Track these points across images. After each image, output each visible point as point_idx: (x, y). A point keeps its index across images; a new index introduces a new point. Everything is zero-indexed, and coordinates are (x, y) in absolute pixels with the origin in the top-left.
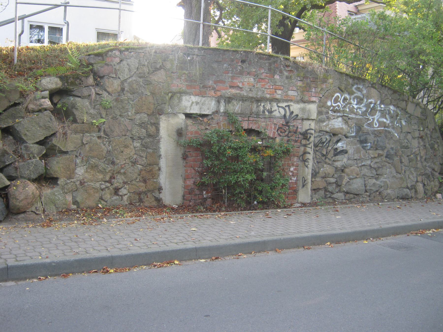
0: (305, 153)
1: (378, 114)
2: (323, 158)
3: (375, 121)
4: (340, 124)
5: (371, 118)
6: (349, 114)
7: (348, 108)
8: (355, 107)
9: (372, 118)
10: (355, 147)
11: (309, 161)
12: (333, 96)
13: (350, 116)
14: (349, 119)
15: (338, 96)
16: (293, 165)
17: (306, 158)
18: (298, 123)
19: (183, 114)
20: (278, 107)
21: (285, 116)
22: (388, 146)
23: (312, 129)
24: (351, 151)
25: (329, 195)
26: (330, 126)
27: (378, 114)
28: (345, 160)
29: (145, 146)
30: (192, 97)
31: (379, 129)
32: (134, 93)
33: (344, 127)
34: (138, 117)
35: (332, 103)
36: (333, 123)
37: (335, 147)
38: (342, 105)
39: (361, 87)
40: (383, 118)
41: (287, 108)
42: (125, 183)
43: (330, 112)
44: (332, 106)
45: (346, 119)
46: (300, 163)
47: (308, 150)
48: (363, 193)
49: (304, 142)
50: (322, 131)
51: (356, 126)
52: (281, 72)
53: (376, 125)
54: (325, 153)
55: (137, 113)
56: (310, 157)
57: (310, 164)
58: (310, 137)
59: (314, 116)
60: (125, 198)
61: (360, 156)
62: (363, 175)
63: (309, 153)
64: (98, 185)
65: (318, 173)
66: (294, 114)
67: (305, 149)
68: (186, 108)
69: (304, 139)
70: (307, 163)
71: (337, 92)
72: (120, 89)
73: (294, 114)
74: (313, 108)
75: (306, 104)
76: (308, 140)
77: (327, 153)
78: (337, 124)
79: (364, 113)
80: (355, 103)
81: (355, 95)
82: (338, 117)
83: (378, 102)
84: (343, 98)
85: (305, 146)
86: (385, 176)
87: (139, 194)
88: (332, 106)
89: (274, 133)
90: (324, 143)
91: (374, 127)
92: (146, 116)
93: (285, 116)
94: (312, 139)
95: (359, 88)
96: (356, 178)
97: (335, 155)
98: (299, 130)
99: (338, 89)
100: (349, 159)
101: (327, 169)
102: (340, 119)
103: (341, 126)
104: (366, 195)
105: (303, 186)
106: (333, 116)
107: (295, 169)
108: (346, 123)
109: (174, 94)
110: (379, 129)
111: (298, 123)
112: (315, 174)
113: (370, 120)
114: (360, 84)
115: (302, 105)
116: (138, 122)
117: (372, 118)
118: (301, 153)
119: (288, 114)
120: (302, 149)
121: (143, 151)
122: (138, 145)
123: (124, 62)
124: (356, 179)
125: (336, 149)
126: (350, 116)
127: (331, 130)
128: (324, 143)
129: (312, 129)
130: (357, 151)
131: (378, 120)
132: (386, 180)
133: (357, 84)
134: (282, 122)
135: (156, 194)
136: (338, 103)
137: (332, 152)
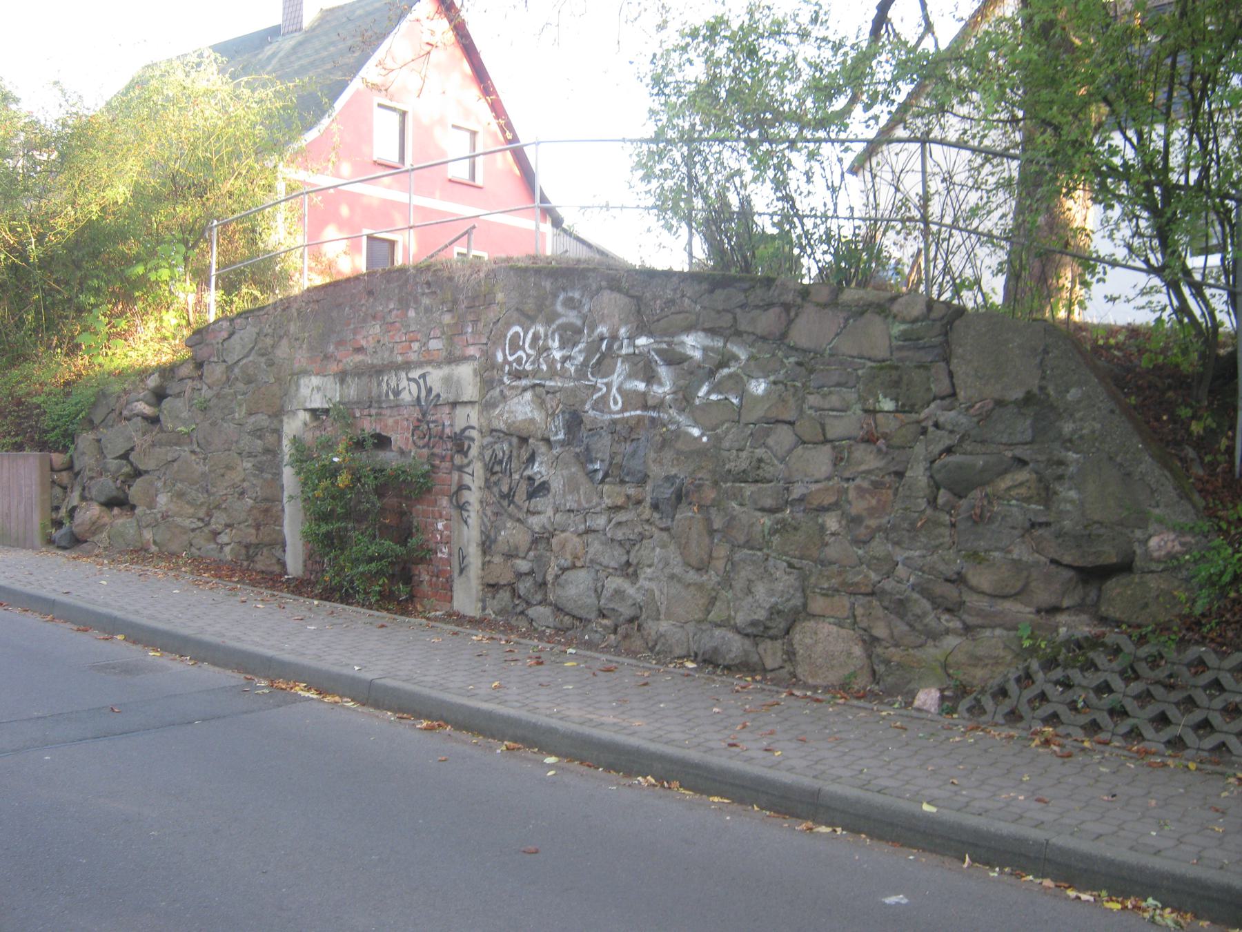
0: (462, 487)
1: (621, 368)
2: (505, 503)
3: (614, 390)
4: (528, 409)
5: (600, 382)
6: (545, 379)
7: (546, 362)
8: (558, 355)
9: (606, 384)
10: (565, 472)
11: (469, 508)
12: (505, 336)
13: (548, 383)
14: (548, 393)
15: (517, 334)
16: (441, 517)
17: (463, 500)
18: (443, 414)
19: (305, 410)
20: (409, 380)
21: (418, 398)
22: (656, 471)
23: (473, 428)
24: (556, 485)
25: (522, 605)
26: (506, 415)
27: (621, 368)
28: (550, 512)
29: (260, 468)
30: (313, 378)
31: (627, 414)
32: (249, 382)
33: (538, 416)
34: (252, 419)
35: (505, 355)
36: (514, 408)
37: (528, 472)
38: (528, 356)
39: (577, 295)
40: (637, 379)
41: (421, 381)
42: (227, 526)
43: (505, 379)
44: (505, 360)
45: (541, 394)
46: (454, 513)
47: (467, 480)
48: (593, 616)
49: (458, 459)
50: (496, 431)
51: (563, 412)
52: (417, 301)
53: (616, 403)
54: (505, 489)
55: (250, 414)
56: (473, 497)
57: (473, 518)
58: (469, 447)
59: (470, 391)
60: (227, 549)
61: (578, 502)
62: (592, 561)
63: (469, 489)
64: (187, 523)
65: (495, 541)
66: (434, 393)
67: (460, 478)
68: (305, 398)
69: (458, 452)
70: (465, 514)
71: (513, 324)
72: (224, 378)
73: (434, 393)
74: (465, 371)
75: (453, 366)
76: (466, 454)
77: (510, 489)
78: (522, 409)
79: (581, 372)
80: (556, 344)
81: (559, 322)
82: (525, 389)
83: (623, 331)
84: (530, 335)
85: (460, 469)
86: (649, 570)
87: (247, 547)
88: (505, 360)
89: (407, 439)
90: (501, 462)
91: (611, 412)
92: (265, 417)
93: (418, 398)
94: (474, 452)
95: (572, 299)
96: (574, 567)
97: (531, 496)
98: (448, 431)
99: (516, 315)
100: (557, 511)
101: (511, 534)
102: (528, 395)
103: (530, 415)
104: (605, 627)
105: (461, 571)
106: (513, 388)
107: (446, 527)
108: (542, 404)
109: (293, 374)
110: (627, 414)
111: (443, 414)
112: (486, 546)
113: (600, 389)
114: (573, 288)
115: (446, 370)
116: (249, 427)
117: (606, 384)
118: (454, 488)
119: (423, 394)
120: (456, 476)
121: (254, 475)
122: (249, 465)
123: (236, 337)
124: (575, 571)
125: (530, 479)
126: (548, 383)
127: (509, 426)
128: (501, 462)
129: (473, 428)
130: (572, 486)
131: (619, 390)
132: (652, 585)
133: (564, 289)
134: (416, 414)
135: (278, 553)
136: (521, 353)
137: (523, 488)
